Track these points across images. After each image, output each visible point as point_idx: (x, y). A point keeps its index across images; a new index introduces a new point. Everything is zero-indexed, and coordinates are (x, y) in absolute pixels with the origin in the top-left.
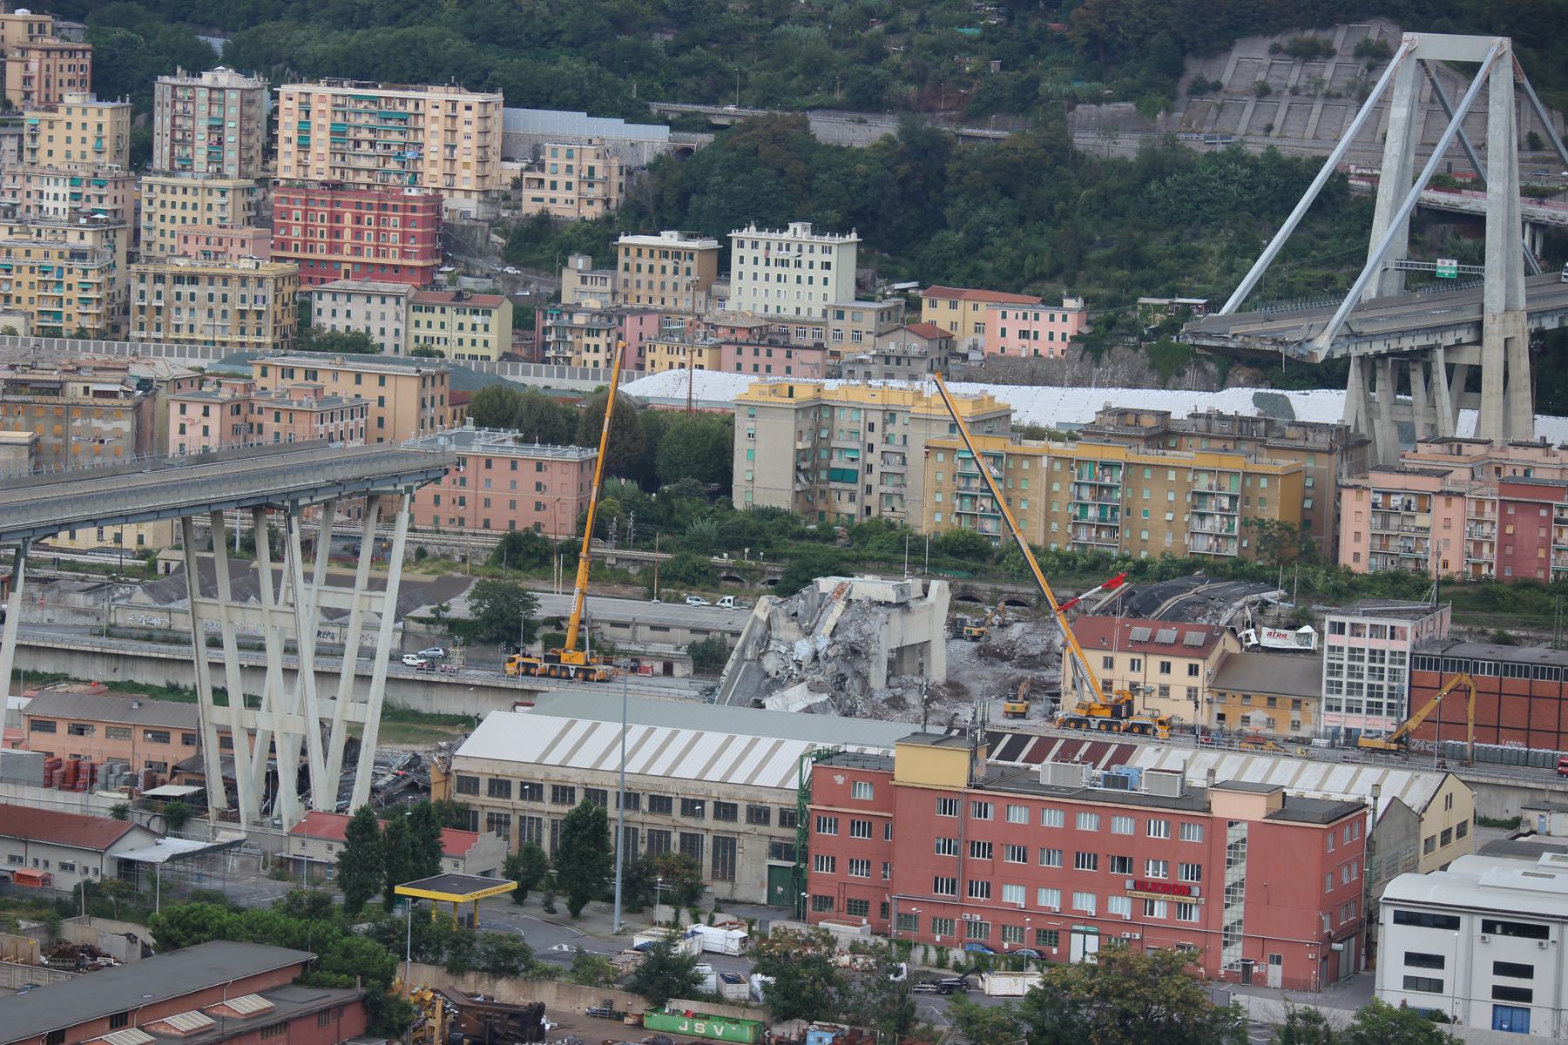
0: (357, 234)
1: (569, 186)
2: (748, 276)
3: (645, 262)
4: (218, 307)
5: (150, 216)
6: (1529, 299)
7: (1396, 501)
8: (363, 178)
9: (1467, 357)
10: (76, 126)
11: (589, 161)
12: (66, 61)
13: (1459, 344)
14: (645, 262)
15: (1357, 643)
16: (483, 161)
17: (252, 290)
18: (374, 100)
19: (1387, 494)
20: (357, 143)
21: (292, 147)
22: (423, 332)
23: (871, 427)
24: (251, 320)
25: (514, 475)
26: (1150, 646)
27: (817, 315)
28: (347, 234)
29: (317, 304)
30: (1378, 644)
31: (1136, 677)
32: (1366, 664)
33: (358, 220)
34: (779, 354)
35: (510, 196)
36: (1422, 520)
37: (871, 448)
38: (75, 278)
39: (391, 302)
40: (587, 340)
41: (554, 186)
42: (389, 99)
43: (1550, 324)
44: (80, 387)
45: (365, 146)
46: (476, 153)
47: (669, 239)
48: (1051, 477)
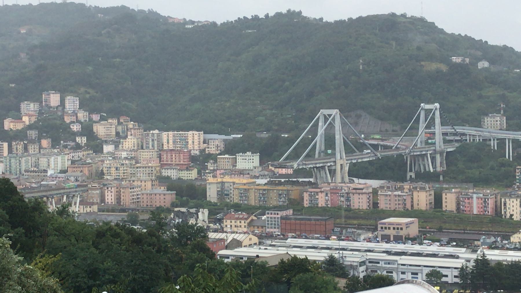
0: (175, 159)
1: (214, 147)
2: (240, 162)
3: (222, 160)
4: (145, 172)
5: (140, 157)
6: (346, 157)
7: (313, 194)
8: (179, 148)
9: (333, 168)
10: (130, 142)
11: (217, 144)
12: (139, 131)
13: (331, 165)
14: (222, 160)
15: (271, 216)
16: (199, 144)
17: (150, 169)
18: (180, 134)
19: (311, 192)
20: (177, 142)
21: (166, 143)
22: (181, 175)
23: (231, 186)
24: (150, 174)
25: (160, 197)
26: (237, 219)
27: (252, 168)
28: (174, 159)
29: (162, 171)
30: (275, 216)
31: (236, 224)
32: (273, 220)
33: (175, 156)
34: (242, 175)
35: (204, 150)
36: (317, 197)
37: (231, 189)
38: (122, 169)
39: (175, 170)
40: (209, 175)
41: (211, 148)
42: (182, 134)
43: (354, 161)
44: (90, 185)
45: (179, 143)
46: (198, 143)
47: (227, 156)
48: (255, 192)
